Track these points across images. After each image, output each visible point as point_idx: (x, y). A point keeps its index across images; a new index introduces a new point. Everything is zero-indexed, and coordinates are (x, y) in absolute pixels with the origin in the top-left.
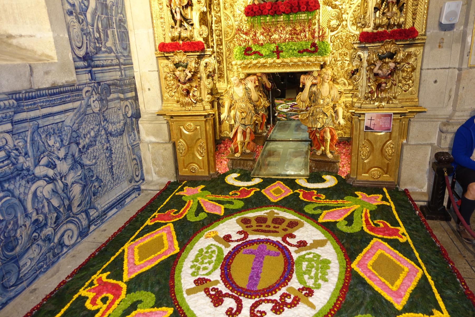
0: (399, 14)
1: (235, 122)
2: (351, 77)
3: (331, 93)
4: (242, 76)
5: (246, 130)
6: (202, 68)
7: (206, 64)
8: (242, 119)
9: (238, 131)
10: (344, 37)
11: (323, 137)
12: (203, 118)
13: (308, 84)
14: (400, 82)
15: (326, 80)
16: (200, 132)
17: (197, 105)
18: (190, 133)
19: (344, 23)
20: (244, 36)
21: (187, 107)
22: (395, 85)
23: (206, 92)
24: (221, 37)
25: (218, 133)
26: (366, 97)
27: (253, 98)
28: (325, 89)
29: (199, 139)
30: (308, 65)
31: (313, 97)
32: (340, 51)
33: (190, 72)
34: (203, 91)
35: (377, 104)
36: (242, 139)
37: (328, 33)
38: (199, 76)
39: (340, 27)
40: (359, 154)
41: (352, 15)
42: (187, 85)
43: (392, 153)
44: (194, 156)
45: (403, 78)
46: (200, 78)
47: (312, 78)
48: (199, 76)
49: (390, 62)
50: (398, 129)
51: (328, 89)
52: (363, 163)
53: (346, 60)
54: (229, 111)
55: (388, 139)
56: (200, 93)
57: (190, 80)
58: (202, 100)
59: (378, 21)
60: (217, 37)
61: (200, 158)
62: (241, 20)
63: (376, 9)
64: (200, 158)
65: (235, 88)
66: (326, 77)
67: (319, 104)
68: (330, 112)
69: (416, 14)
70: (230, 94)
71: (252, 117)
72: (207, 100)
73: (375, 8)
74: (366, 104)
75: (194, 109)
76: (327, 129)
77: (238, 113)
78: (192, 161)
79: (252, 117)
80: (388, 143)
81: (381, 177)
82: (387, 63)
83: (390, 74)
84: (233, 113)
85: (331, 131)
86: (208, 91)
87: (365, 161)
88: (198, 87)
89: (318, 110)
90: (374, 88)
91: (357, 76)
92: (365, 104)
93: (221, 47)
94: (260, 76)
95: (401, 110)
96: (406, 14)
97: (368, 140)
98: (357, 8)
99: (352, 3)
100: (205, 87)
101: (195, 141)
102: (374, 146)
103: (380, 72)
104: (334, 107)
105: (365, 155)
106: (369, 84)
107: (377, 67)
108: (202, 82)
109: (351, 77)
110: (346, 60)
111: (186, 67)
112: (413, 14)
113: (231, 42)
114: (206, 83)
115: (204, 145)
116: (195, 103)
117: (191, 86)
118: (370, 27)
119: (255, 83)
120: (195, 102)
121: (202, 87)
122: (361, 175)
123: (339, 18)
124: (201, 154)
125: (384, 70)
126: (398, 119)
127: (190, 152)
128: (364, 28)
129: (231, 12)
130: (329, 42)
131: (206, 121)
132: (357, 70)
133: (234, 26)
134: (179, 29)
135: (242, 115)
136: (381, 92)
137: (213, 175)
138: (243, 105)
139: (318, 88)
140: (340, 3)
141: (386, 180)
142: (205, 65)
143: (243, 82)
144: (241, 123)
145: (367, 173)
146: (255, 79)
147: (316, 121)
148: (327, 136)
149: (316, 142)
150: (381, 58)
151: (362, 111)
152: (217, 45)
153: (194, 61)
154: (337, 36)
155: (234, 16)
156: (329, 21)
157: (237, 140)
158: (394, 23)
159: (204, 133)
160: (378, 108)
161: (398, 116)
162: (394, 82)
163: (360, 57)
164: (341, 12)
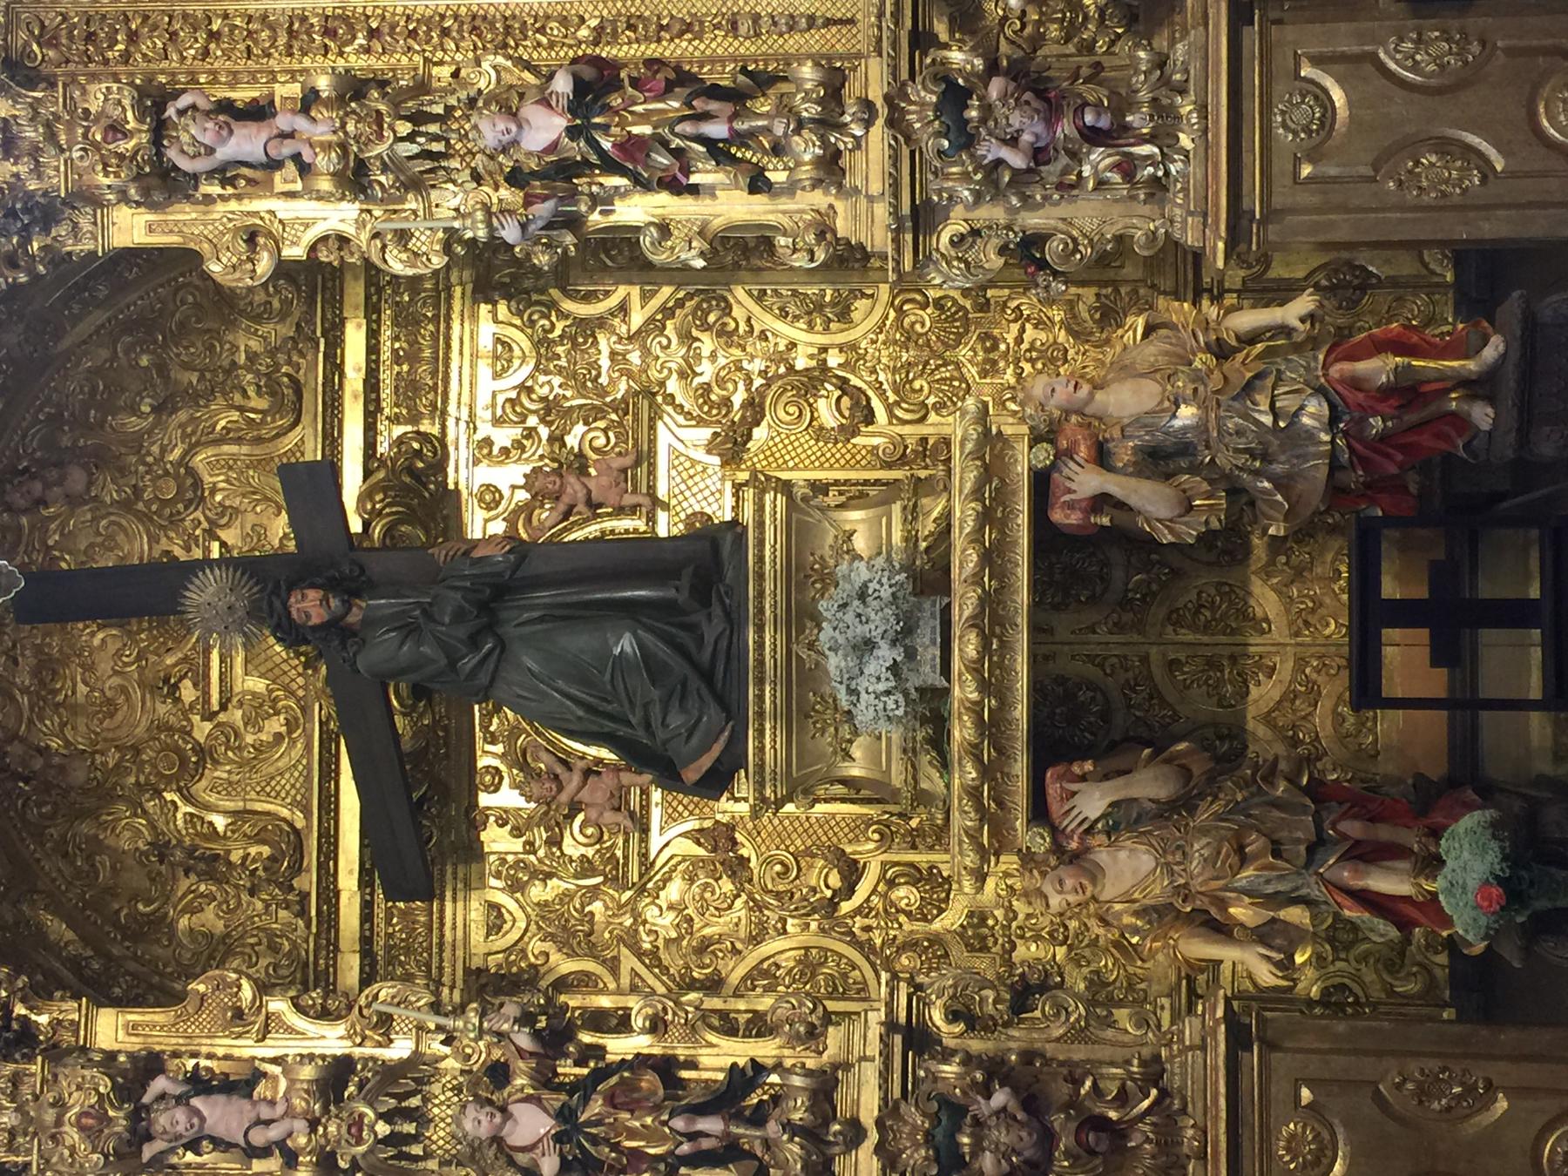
0: (784, 87)
4: (1039, 842)
5: (1344, 837)
10: (905, 356)
14: (1089, 47)
18: (1341, 1138)
19: (834, 359)
20: (863, 890)
21: (1186, 1150)
26: (1150, 196)
29: (1378, 1097)
30: (1003, 496)
32: (971, 372)
33: (988, 1097)
36: (1404, 865)
37: (873, 435)
39: (855, 381)
40: (1456, 200)
41: (802, 324)
43: (1447, 41)
45: (1067, 40)
52: (1509, 174)
53: (1019, 340)
55: (1368, 68)
57: (1032, 1103)
59: (806, 173)
62: (778, 895)
63: (758, 184)
64: (1502, 1105)
65: (1109, 891)
69: (792, 16)
71: (1276, 804)
73: (753, 189)
74: (1185, 190)
79: (1276, 804)
80: (1392, 66)
82: (987, 109)
83: (1041, 94)
84: (1241, 912)
87: (1499, 168)
92: (1187, 196)
95: (1217, 26)
96: (787, 60)
98: (769, 301)
99: (743, 328)
102: (1410, 129)
104: (1221, 351)
106: (1091, 185)
107: (1005, 153)
108: (1050, 1049)
110: (1019, 340)
112: (791, 29)
115: (1413, 1067)
118: (831, 206)
119: (1083, 778)
121: (1079, 1053)
123: (810, 383)
128: (834, 232)
129: (735, 951)
133: (804, 939)
134: (773, 1128)
138: (1199, 848)
140: (741, 386)
142: (959, 1028)
143: (1074, 845)
144: (1302, 860)
146: (1060, 778)
149: (1426, 440)
150: (965, 139)
151: (1217, 205)
154: (896, 392)
155: (755, 940)
156: (820, 433)
157: (1406, 899)
158: (819, 102)
160: (1205, 131)
161: (1252, 36)
162: (1085, 71)
163: (962, 237)
164: (781, 377)
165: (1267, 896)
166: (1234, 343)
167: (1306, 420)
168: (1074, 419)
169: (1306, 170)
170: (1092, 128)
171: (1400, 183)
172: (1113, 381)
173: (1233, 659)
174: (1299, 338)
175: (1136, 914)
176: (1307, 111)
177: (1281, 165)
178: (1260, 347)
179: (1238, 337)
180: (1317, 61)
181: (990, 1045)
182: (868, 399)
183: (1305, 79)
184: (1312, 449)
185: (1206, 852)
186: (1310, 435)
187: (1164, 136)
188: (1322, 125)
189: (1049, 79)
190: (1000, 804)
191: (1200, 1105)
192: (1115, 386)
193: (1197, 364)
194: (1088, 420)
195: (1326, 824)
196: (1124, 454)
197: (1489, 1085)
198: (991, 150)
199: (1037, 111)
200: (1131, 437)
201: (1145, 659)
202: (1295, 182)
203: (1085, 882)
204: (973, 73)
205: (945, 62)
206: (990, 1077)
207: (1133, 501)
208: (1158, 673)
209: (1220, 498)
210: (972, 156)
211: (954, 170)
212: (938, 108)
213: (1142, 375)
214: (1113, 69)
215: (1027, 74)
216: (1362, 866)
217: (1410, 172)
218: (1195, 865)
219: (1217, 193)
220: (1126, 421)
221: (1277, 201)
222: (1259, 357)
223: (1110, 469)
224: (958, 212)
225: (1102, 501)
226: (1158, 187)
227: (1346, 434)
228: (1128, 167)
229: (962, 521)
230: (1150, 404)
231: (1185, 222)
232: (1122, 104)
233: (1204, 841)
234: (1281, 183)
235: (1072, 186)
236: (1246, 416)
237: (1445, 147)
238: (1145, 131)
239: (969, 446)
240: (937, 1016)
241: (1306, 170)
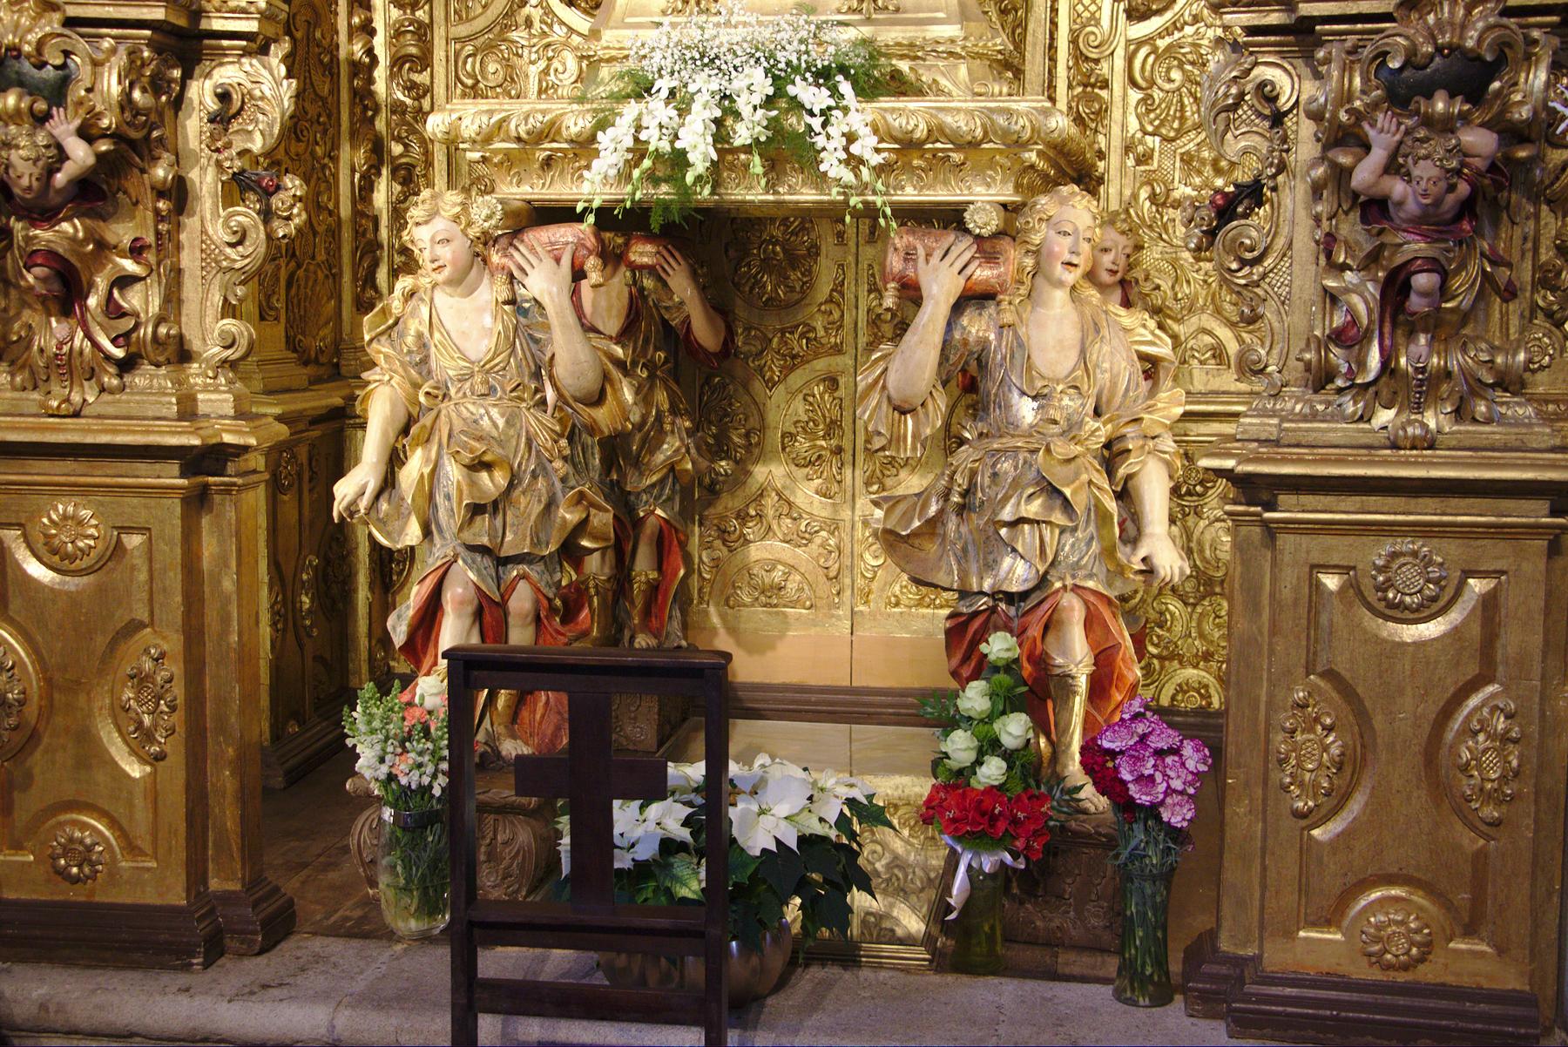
1: (427, 533)
2: (1211, 234)
3: (1093, 356)
6: (193, 127)
7: (224, 97)
8: (476, 510)
9: (450, 597)
11: (1041, 662)
12: (170, 476)
13: (941, 283)
16: (143, 576)
17: (138, 380)
18: (72, 583)
21: (56, 388)
22: (1510, 293)
23: (217, 299)
24: (420, 14)
25: (363, 642)
27: (560, 370)
28: (1053, 329)
29: (135, 627)
31: (970, 381)
34: (190, 290)
35: (1385, 416)
37: (1113, 18)
38: (160, 172)
40: (1275, 776)
42: (66, 227)
43: (1503, 777)
44: (90, 755)
46: (179, 194)
47: (964, 249)
48: (160, 172)
49: (1464, 118)
50: (1538, 603)
51: (1071, 334)
52: (1308, 848)
54: (394, 460)
55: (1472, 670)
56: (173, 299)
57: (93, 194)
58: (183, 354)
60: (395, 13)
61: (135, 770)
64: (135, 770)
65: (443, 299)
66: (1062, 247)
67: (1010, 426)
68: (1087, 485)
70: (410, 340)
71: (550, 505)
72: (215, 351)
74: (1314, 416)
75: (108, 404)
77: (453, 472)
78: (69, 792)
79: (550, 505)
80: (1474, 701)
81: (1438, 957)
82: (1446, 126)
83: (1467, 208)
84: (414, 468)
85: (1091, 622)
86: (225, 288)
87: (1315, 832)
88: (161, 250)
89: (1006, 466)
90: (1361, 308)
91: (1253, 227)
92: (1305, 419)
93: (422, 78)
94: (651, 269)
97: (1330, 675)
100: (210, 258)
101: (101, 642)
102: (1379, 722)
103: (1397, 188)
104: (1112, 455)
105: (1316, 785)
106: (1330, 283)
107: (1378, 156)
108: (191, 223)
109: (1211, 234)
111: (58, 93)
113: (490, 48)
114: (219, 233)
115: (174, 668)
116: (126, 366)
117: (103, 247)
120: (119, 353)
121: (189, 260)
122: (1290, 935)
124: (140, 740)
125: (1425, 171)
126: (1534, 530)
127: (59, 720)
130: (1118, 83)
131: (197, 501)
132: (1253, 193)
135: (473, 484)
136: (1411, 335)
137: (227, 898)
138: (492, 417)
139: (1008, 318)
141: (1466, 981)
142: (212, 105)
143: (495, 258)
144: (469, 537)
145: (1327, 922)
147: (990, 546)
148: (1065, 653)
151: (1285, 460)
152: (398, 62)
153: (121, 59)
154: (1169, 47)
159: (175, 579)
160: (1395, 446)
161: (1536, 513)
162: (1503, 274)
163: (1272, 99)
165: (431, 496)
166: (1122, 472)
167: (1007, 561)
169: (1331, 582)
170: (1406, 288)
171: (1303, 706)
173: (839, 451)
174: (1122, 553)
175: (420, 336)
176: (1411, 584)
177: (1340, 548)
178: (1112, 505)
179: (1129, 477)
180: (1489, 603)
181: (193, 143)
182: (1159, 12)
183: (1462, 584)
184: (974, 567)
185: (485, 422)
186: (990, 566)
187: (1392, 385)
188: (1391, 605)
189: (1496, 224)
190: (548, 163)
191: (111, 410)
193: (1091, 424)
195: (524, 568)
196: (976, 326)
197: (159, 757)
198: (1383, 134)
199: (1438, 203)
201: (838, 350)
202: (1313, 567)
203: (446, 272)
204: (1506, 106)
205: (1529, 60)
206: (116, 136)
207: (910, 338)
208: (821, 365)
210: (1375, 106)
211: (1357, 81)
212: (1455, 49)
213: (1083, 352)
214: (1505, 316)
215: (1499, 187)
216: (470, 609)
217: (1317, 720)
218: (472, 409)
219: (1300, 461)
221: (1286, 541)
222: (1098, 505)
223: (958, 308)
224: (1309, 89)
225: (912, 294)
226: (1320, 378)
227: (993, 610)
228: (1349, 337)
229: (900, 112)
230: (1039, 361)
231: (1273, 413)
232: (1443, 328)
233: (501, 422)
234: (1314, 547)
235: (1329, 255)
236: (1016, 484)
237: (1350, 768)
238: (1403, 361)
239: (1001, 121)
240: (229, 73)
241: (1331, 582)
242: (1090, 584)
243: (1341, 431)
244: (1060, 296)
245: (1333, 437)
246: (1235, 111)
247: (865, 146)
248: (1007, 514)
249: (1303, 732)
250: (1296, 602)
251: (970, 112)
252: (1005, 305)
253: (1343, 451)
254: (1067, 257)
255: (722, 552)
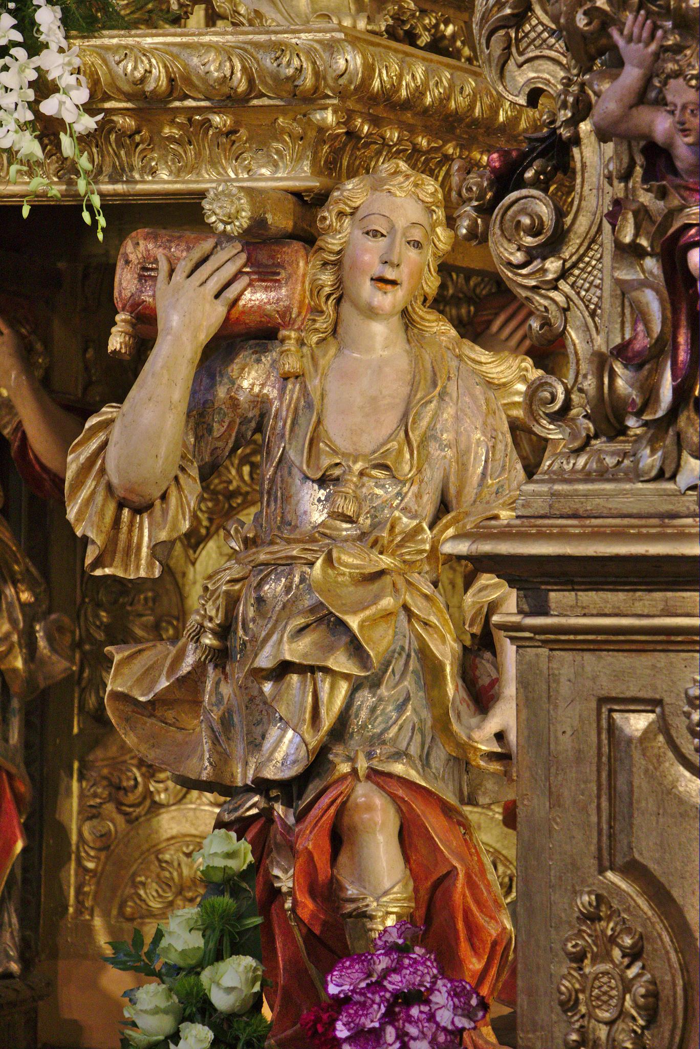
11: (328, 893)
13: (188, 314)
15: (367, 291)
51: (394, 388)
66: (369, 254)
67: (287, 523)
74: (603, 475)
76: (363, 792)
85: (409, 836)
92: (587, 477)
139: (291, 364)
168: (327, 278)
172: (416, 360)
192: (403, 363)
194: (329, 308)
200: (282, 391)
202: (603, 701)
209: (150, 566)
217: (613, 940)
219: (563, 536)
220: (314, 384)
229: (127, 52)
234: (605, 671)
239: (268, 62)
241: (638, 723)
242: (399, 768)
243: (642, 495)
244: (379, 330)
245: (616, 504)
246: (519, 27)
247: (67, 105)
248: (265, 660)
249: (594, 962)
250: (579, 757)
251: (226, 52)
252: (291, 345)
253: (626, 521)
254: (377, 270)
255: (114, 823)
